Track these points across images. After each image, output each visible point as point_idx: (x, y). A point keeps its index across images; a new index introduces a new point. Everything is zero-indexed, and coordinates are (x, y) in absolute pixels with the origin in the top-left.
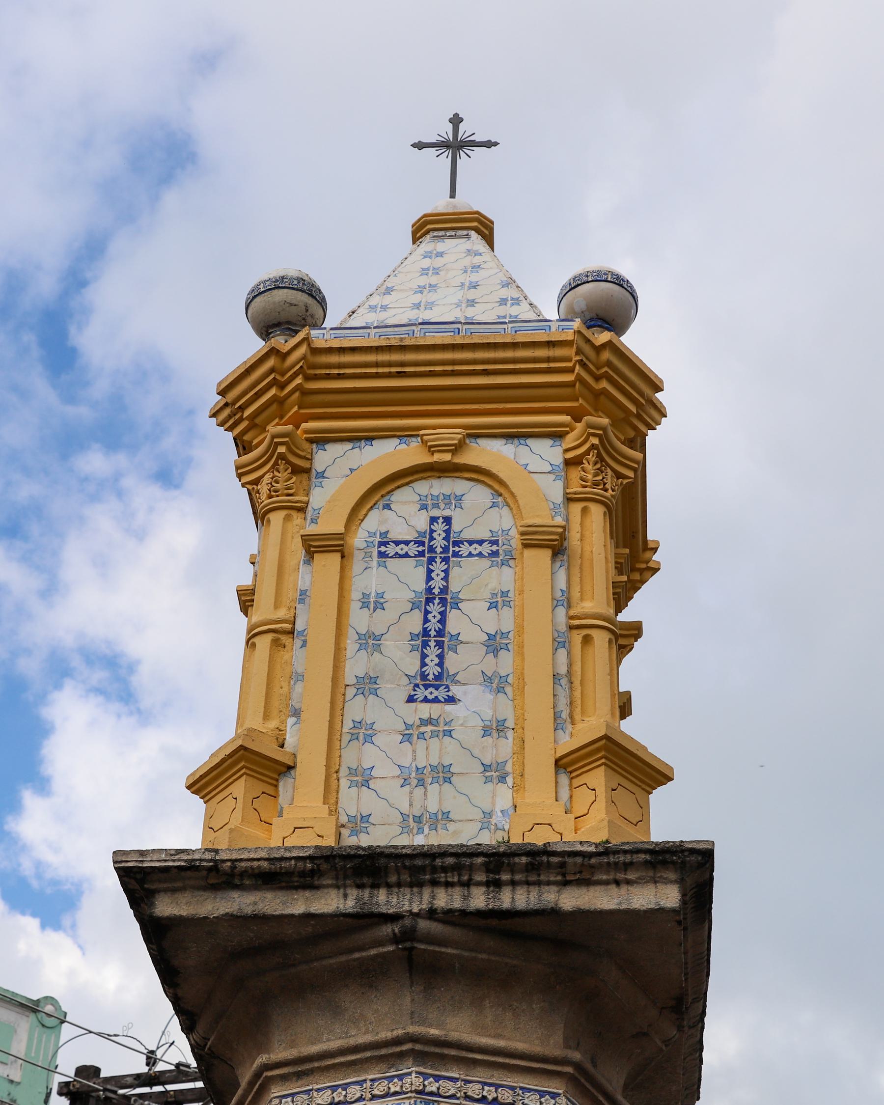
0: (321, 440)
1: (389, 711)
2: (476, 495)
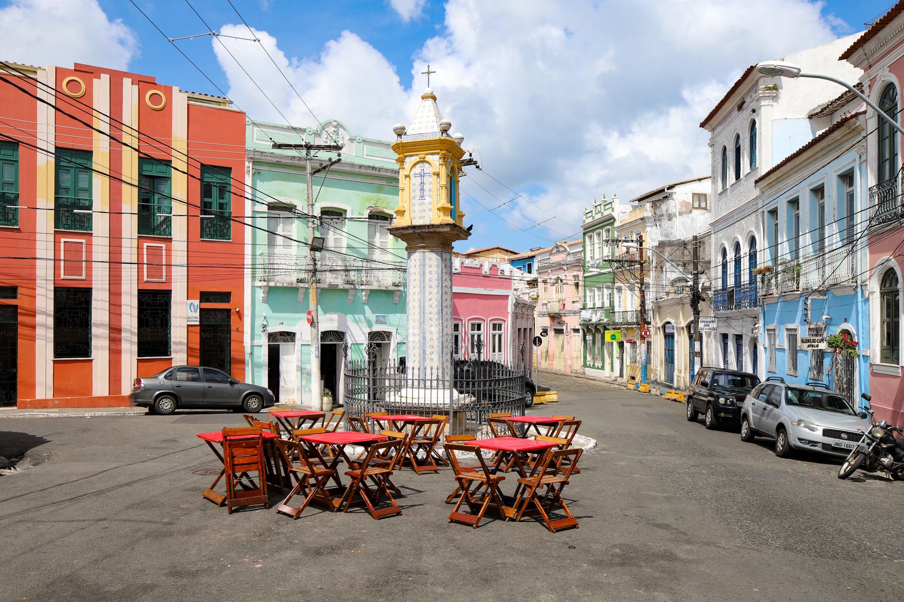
0: (406, 157)
1: (417, 201)
2: (427, 165)
